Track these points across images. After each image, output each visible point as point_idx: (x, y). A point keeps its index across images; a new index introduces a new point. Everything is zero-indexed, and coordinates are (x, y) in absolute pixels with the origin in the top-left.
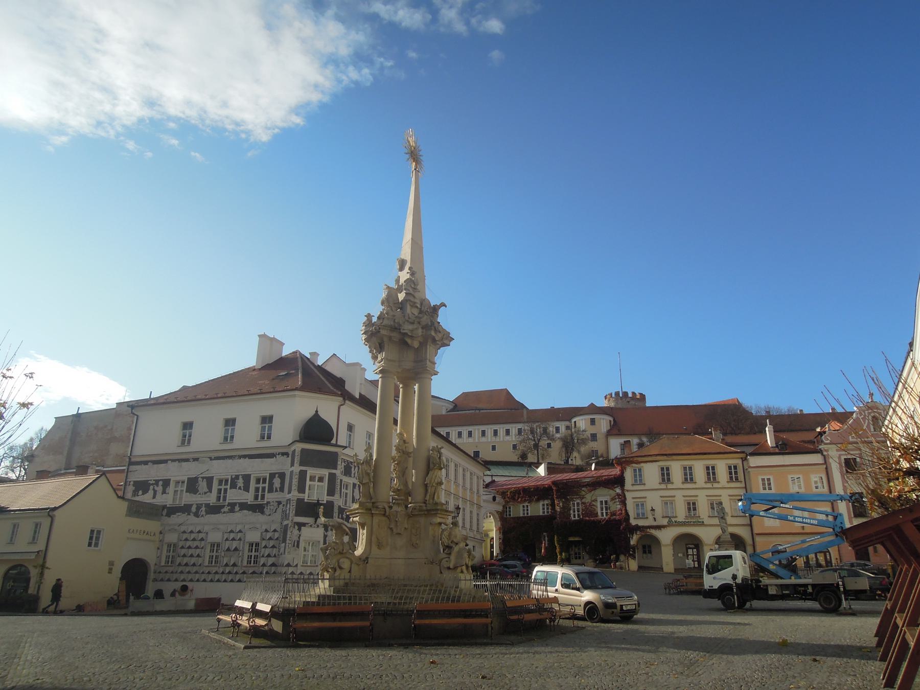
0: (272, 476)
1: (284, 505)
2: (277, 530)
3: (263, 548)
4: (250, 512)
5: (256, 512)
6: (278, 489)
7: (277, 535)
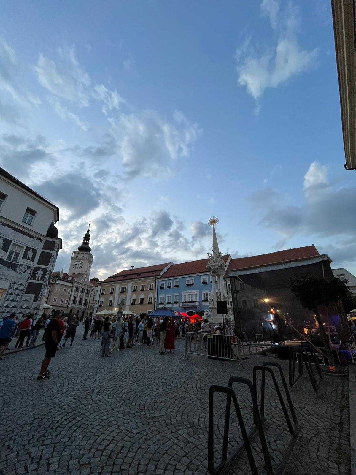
0: (28, 249)
1: (31, 270)
2: (23, 284)
3: (10, 294)
4: (4, 267)
5: (9, 268)
6: (30, 259)
7: (22, 287)
